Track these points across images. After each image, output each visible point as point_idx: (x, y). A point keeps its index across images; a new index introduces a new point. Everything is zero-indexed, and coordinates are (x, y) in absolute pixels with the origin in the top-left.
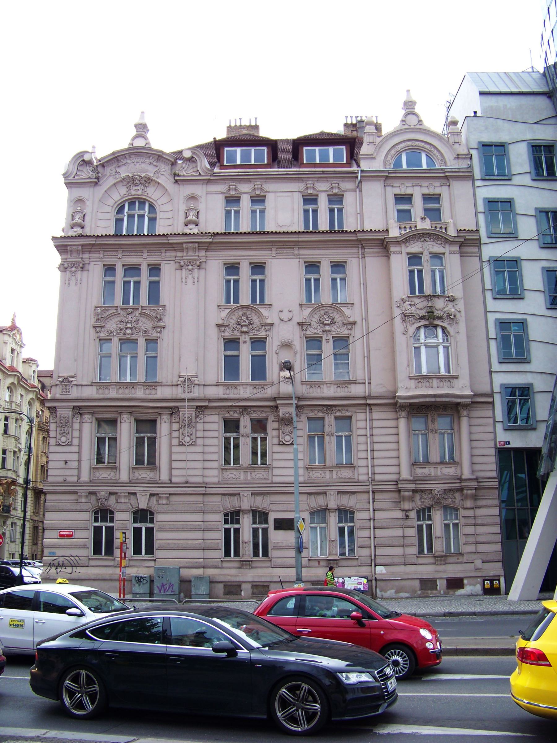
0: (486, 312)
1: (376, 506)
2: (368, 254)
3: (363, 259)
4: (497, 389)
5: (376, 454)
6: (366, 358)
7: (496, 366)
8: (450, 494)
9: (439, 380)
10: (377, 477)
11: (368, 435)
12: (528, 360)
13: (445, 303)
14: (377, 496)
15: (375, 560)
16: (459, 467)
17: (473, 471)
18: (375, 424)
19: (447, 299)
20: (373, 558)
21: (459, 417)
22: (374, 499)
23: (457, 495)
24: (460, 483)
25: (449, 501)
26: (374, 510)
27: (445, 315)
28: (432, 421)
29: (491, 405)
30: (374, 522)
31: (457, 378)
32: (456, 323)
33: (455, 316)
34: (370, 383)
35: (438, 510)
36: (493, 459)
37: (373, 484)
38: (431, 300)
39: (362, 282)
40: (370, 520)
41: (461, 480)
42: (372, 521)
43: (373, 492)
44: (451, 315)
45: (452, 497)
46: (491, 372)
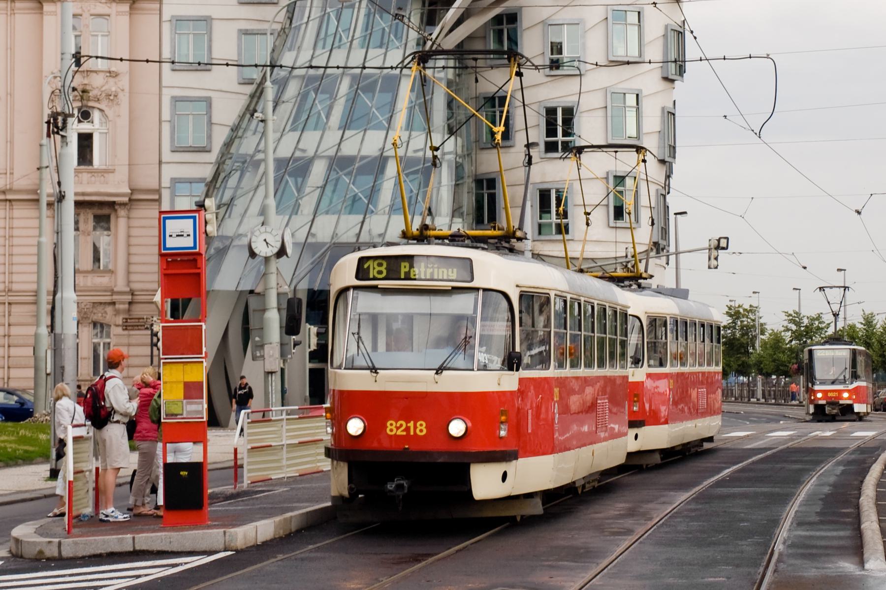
0: (160, 87)
1: (12, 320)
2: (20, 9)
3: (12, 15)
4: (166, 183)
5: (15, 259)
6: (9, 144)
7: (167, 156)
8: (100, 308)
9: (90, 175)
10: (15, 287)
11: (7, 237)
12: (207, 149)
13: (104, 79)
14: (14, 309)
15: (8, 383)
16: (113, 275)
17: (129, 282)
18: (16, 223)
19: (108, 74)
20: (6, 380)
21: (117, 217)
22: (9, 312)
23: (109, 309)
24: (112, 295)
25: (97, 317)
26: (9, 325)
27: (104, 95)
28: (85, 222)
29: (158, 203)
30: (8, 339)
31: (113, 172)
32: (118, 104)
33: (116, 96)
34: (12, 174)
35: (85, 326)
36: (156, 268)
37: (9, 294)
38: (88, 76)
39: (9, 46)
40: (5, 336)
41: (113, 292)
42: (6, 337)
43: (10, 304)
44: (111, 95)
45: (103, 312)
46: (160, 162)
